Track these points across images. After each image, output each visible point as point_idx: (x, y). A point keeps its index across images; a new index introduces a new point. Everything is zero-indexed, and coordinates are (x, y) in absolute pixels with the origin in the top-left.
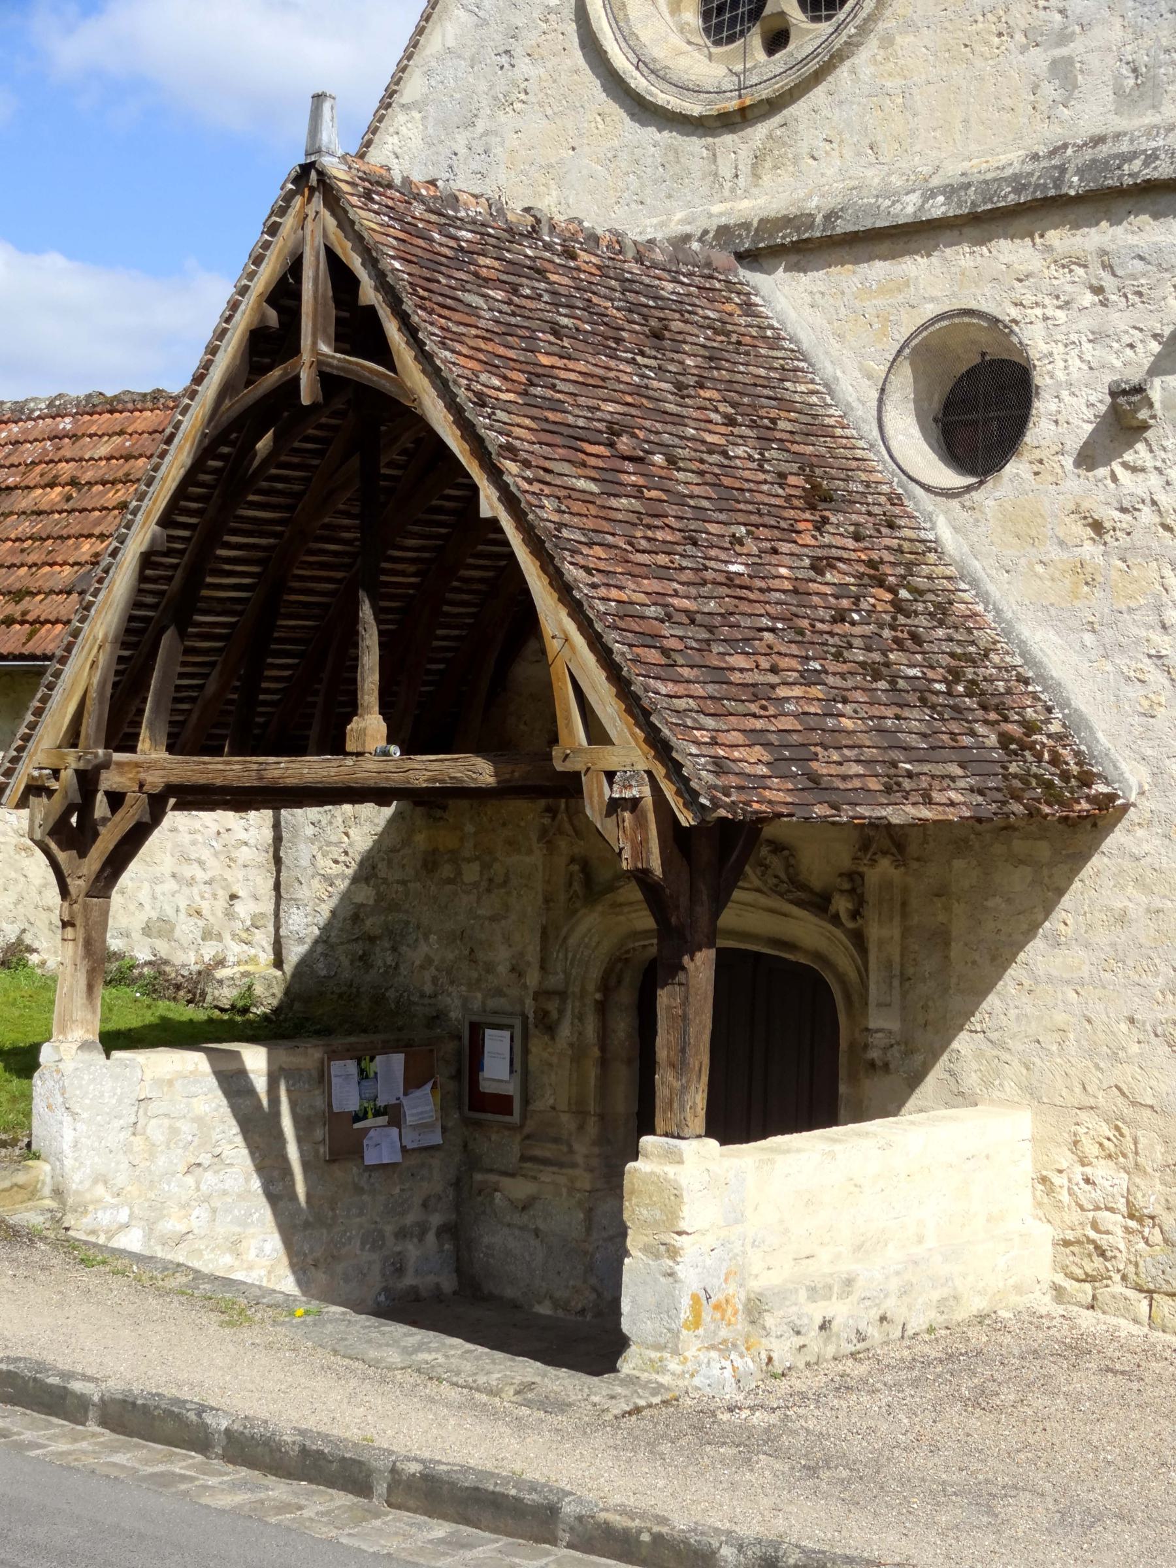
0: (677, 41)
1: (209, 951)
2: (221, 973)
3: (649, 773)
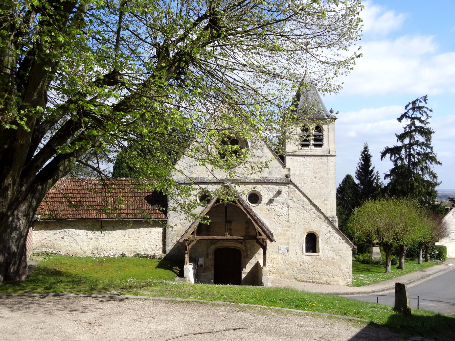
1: (153, 252)
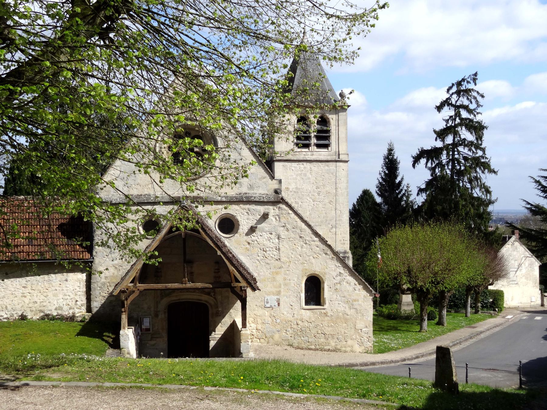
1: (71, 312)
2: (77, 315)
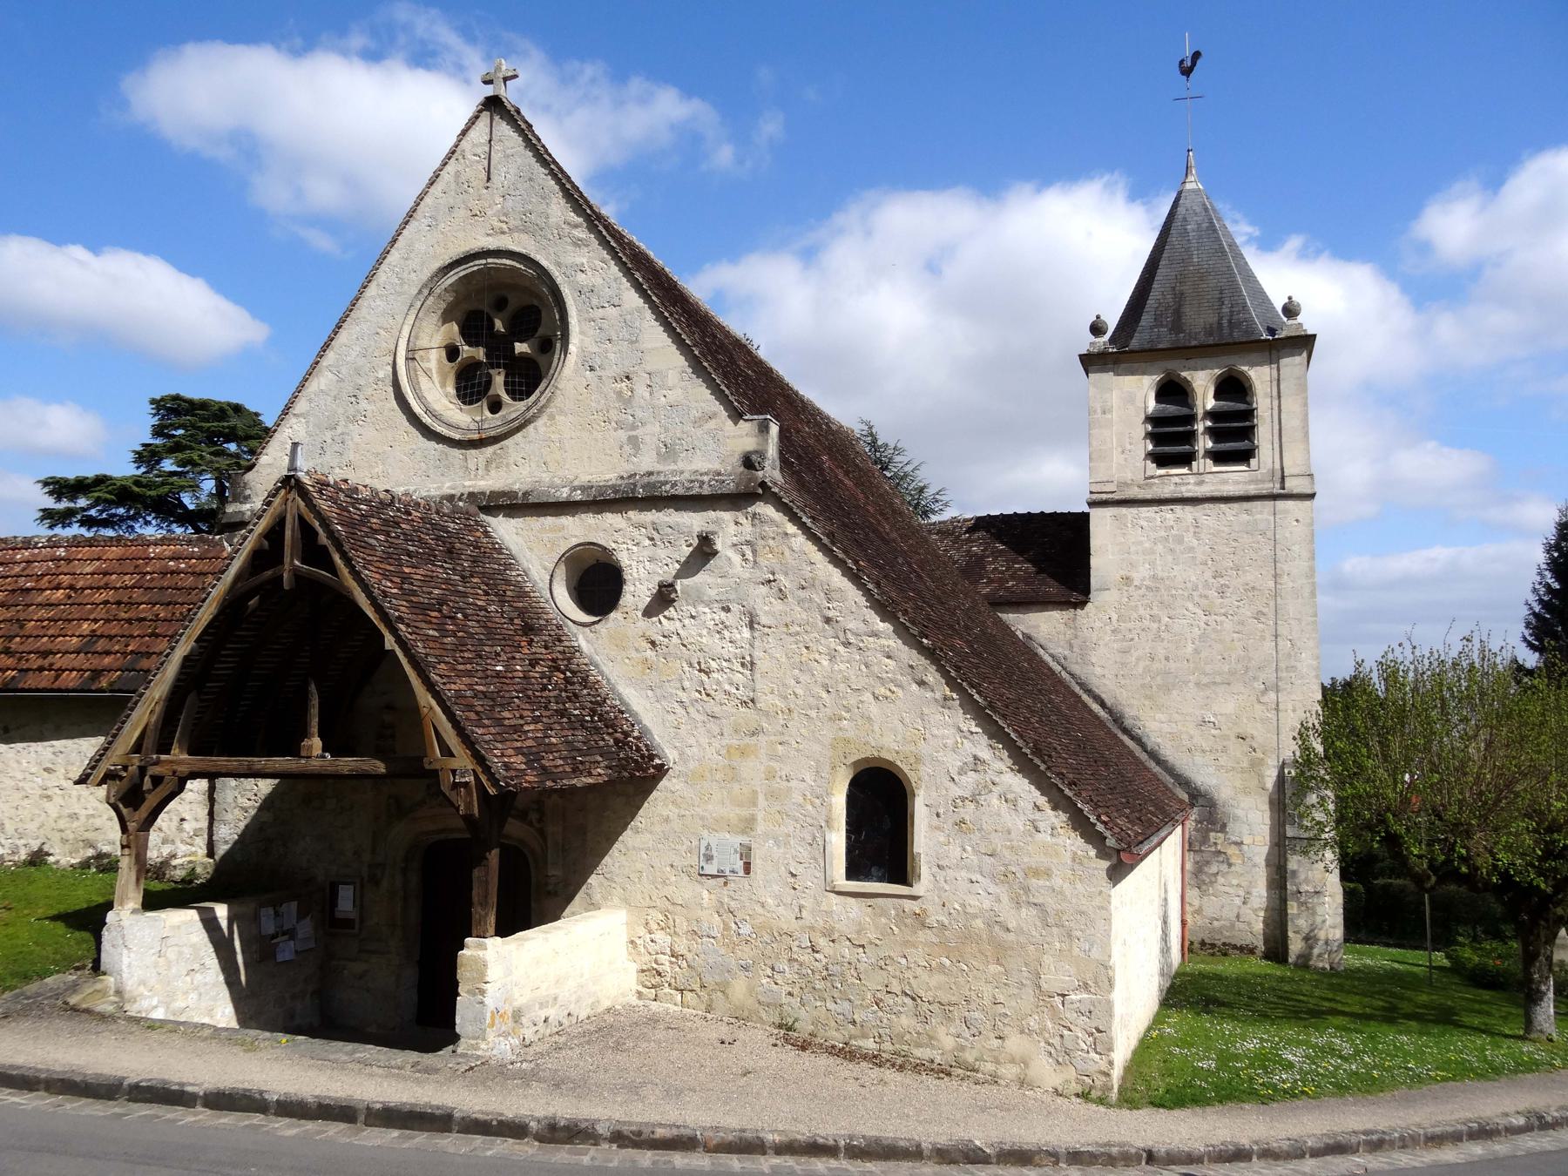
0: (445, 401)
1: (166, 850)
2: (174, 862)
3: (473, 770)
